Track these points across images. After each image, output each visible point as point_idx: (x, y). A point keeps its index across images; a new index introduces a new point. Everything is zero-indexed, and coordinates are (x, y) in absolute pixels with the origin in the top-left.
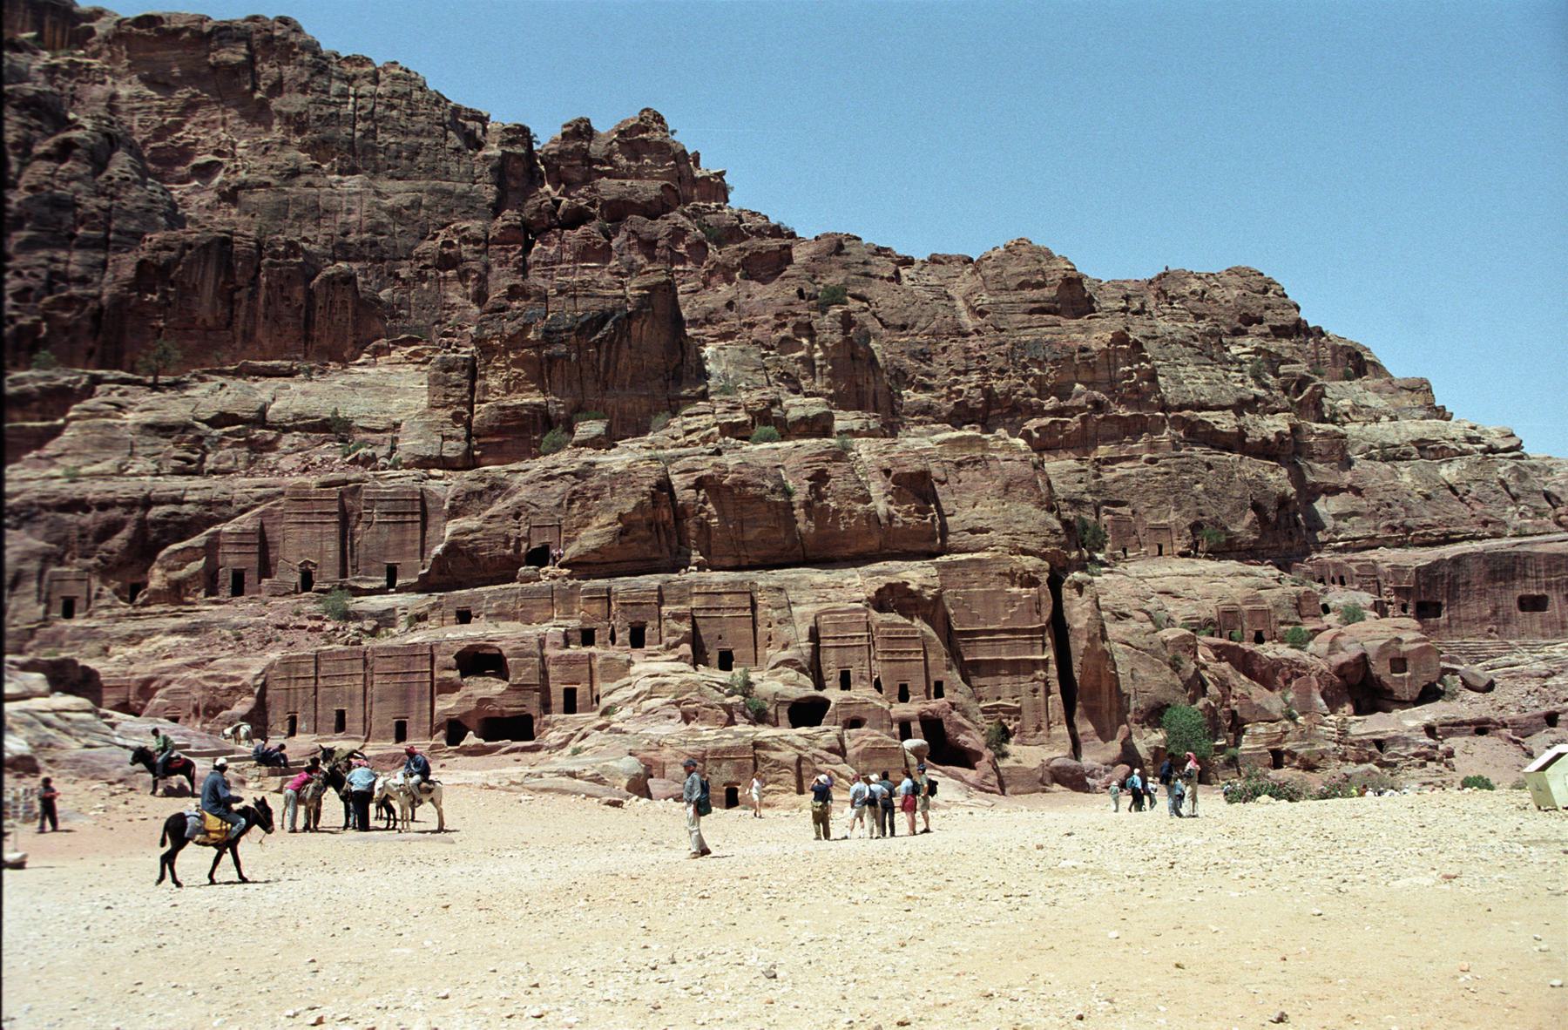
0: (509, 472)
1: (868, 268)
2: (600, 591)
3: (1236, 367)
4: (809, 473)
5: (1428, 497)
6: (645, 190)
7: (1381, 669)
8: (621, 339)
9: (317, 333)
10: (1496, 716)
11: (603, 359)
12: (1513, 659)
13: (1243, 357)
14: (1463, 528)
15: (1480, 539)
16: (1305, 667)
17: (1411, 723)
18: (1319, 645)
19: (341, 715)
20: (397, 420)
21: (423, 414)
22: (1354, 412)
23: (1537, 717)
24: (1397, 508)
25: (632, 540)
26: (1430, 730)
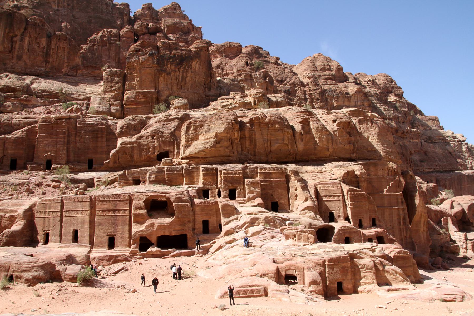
0: (147, 118)
1: (266, 59)
2: (212, 169)
4: (300, 119)
6: (182, 23)
8: (188, 68)
9: (51, 60)
11: (181, 76)
19: (76, 233)
20: (89, 96)
21: (101, 94)
25: (221, 147)
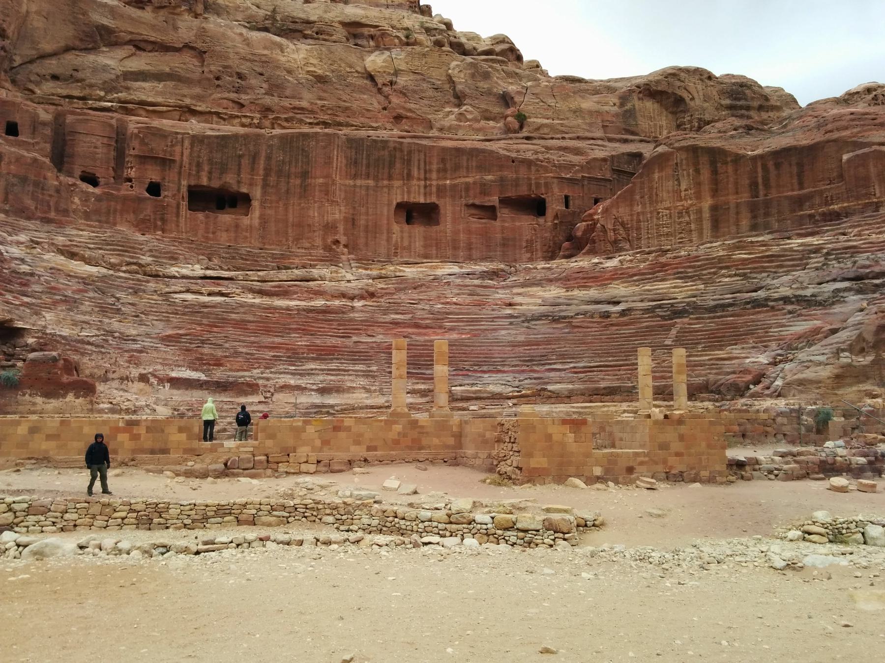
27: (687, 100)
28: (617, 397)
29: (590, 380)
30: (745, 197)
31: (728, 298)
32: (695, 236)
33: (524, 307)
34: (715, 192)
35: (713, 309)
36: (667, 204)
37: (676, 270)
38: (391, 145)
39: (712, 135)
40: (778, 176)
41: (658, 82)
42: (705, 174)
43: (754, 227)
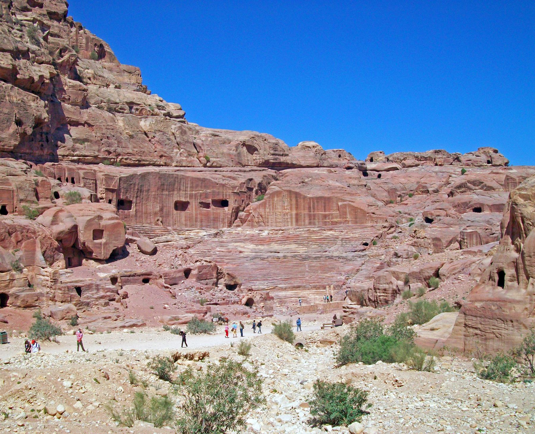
3: (18, 27)
5: (131, 137)
7: (85, 237)
10: (155, 271)
12: (169, 237)
13: (24, 22)
14: (149, 158)
15: (159, 165)
16: (34, 233)
17: (102, 275)
18: (46, 218)
22: (94, 78)
23: (180, 271)
24: (113, 141)
26: (114, 280)
27: (259, 150)
28: (301, 289)
29: (290, 283)
30: (306, 212)
31: (318, 255)
32: (290, 223)
33: (246, 253)
34: (297, 208)
35: (316, 258)
36: (280, 211)
37: (293, 241)
38: (175, 176)
39: (293, 185)
40: (318, 206)
41: (248, 140)
42: (294, 202)
43: (310, 223)
